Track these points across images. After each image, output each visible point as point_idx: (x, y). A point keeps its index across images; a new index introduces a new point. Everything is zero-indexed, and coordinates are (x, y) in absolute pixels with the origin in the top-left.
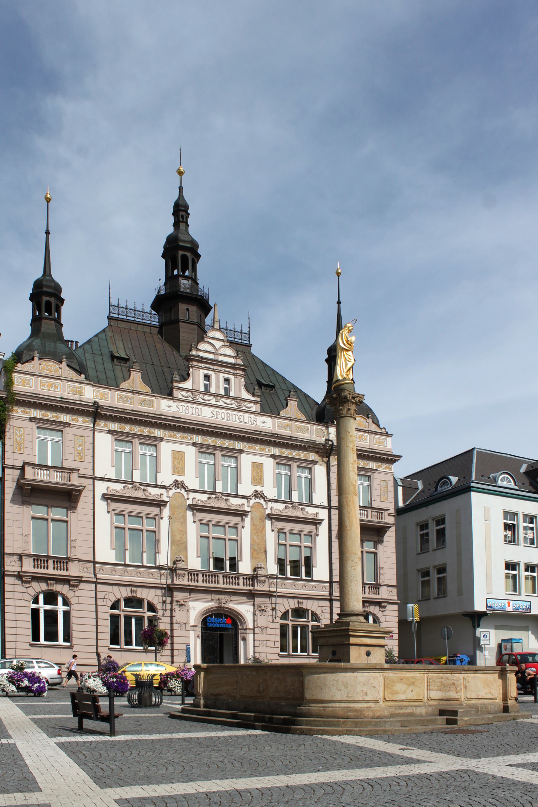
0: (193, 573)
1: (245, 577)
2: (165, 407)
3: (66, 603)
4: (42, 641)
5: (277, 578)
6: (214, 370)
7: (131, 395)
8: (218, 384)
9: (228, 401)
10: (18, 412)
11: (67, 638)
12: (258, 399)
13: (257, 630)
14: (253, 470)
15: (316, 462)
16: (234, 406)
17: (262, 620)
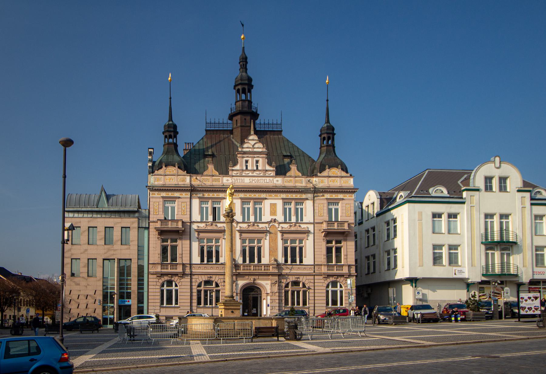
1: (266, 265)
2: (226, 180)
3: (176, 286)
4: (165, 305)
5: (284, 265)
7: (209, 178)
9: (258, 172)
11: (176, 303)
16: (261, 175)
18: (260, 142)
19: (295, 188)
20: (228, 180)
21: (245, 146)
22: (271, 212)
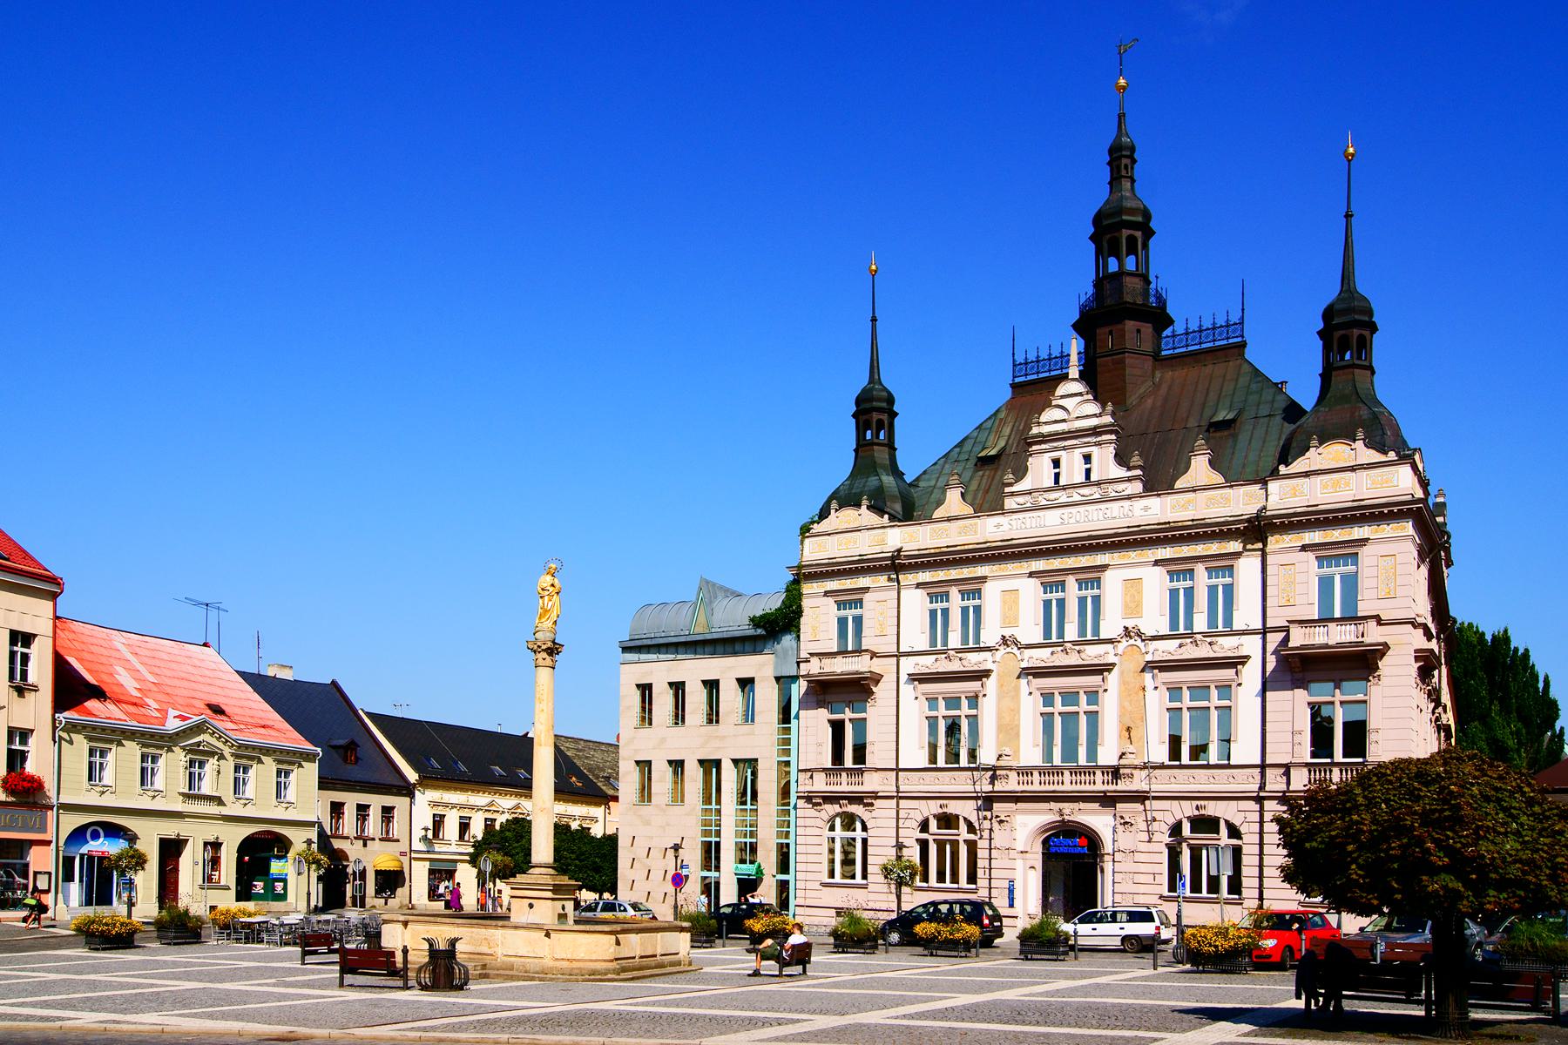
0: (1025, 771)
6: (1064, 448)
8: (1073, 469)
10: (807, 588)
12: (1138, 472)
13: (1118, 856)
14: (1126, 592)
15: (1238, 555)
16: (1097, 496)
17: (1126, 840)
18: (1096, 399)
19: (1198, 524)
20: (998, 526)
21: (1048, 415)
22: (1126, 606)
